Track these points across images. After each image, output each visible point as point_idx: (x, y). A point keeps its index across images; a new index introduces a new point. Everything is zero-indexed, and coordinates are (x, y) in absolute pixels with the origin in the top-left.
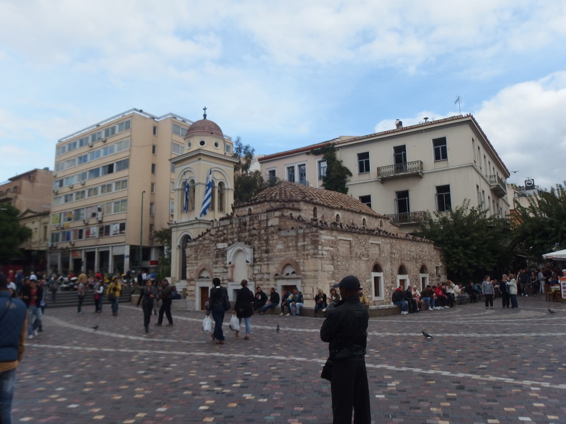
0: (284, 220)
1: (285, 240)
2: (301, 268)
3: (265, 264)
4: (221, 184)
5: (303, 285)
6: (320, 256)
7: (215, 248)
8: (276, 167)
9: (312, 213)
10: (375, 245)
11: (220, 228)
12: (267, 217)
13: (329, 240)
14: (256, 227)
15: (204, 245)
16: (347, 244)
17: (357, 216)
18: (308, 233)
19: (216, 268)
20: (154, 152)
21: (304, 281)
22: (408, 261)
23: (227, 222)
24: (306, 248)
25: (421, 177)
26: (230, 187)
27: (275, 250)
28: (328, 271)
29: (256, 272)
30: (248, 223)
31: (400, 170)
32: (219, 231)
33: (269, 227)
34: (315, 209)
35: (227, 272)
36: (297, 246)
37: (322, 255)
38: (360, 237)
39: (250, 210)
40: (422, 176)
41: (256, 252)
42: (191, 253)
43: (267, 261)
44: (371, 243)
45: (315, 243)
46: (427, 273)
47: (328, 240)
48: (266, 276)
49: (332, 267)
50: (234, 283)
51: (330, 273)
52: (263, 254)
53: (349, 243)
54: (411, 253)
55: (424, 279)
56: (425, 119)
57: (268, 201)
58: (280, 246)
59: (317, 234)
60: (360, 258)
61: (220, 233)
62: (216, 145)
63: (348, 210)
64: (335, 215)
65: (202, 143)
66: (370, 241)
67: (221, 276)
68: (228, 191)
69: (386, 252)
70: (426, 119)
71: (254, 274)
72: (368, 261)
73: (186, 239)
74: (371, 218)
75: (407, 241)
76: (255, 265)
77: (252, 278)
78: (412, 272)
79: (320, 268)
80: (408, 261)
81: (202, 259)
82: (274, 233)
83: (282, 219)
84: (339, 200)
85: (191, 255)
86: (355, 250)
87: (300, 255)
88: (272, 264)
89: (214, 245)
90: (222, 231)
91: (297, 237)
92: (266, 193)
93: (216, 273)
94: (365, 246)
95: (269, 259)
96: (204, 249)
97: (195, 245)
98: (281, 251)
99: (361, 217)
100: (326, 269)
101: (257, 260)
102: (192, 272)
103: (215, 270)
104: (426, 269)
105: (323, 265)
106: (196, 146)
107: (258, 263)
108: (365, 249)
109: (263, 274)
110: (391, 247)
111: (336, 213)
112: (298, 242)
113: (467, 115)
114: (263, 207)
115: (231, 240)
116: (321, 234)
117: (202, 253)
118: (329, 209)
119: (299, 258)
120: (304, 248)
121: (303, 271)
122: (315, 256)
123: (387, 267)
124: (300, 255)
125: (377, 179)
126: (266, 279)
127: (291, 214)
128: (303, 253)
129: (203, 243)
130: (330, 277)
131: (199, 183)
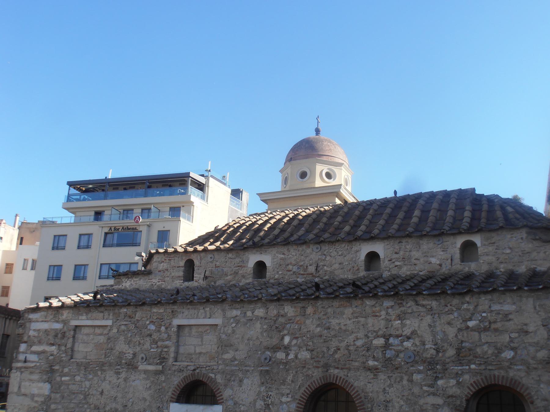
6: (19, 365)
13: (46, 332)
28: (33, 396)
38: (139, 314)
44: (179, 327)
51: (36, 399)
66: (177, 322)
79: (16, 390)
80: (374, 370)
86: (117, 348)
105: (23, 384)
111: (253, 258)
116: (30, 321)
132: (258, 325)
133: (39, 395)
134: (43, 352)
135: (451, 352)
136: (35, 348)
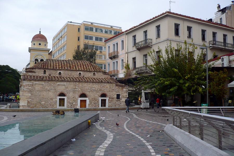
9: (43, 73)
20: (79, 40)
25: (151, 47)
28: (27, 96)
37: (24, 90)
62: (40, 44)
66: (57, 84)
79: (22, 95)
80: (89, 92)
116: (23, 82)
127: (45, 72)
132: (72, 85)
134: (28, 88)
135: (99, 90)
136: (25, 87)
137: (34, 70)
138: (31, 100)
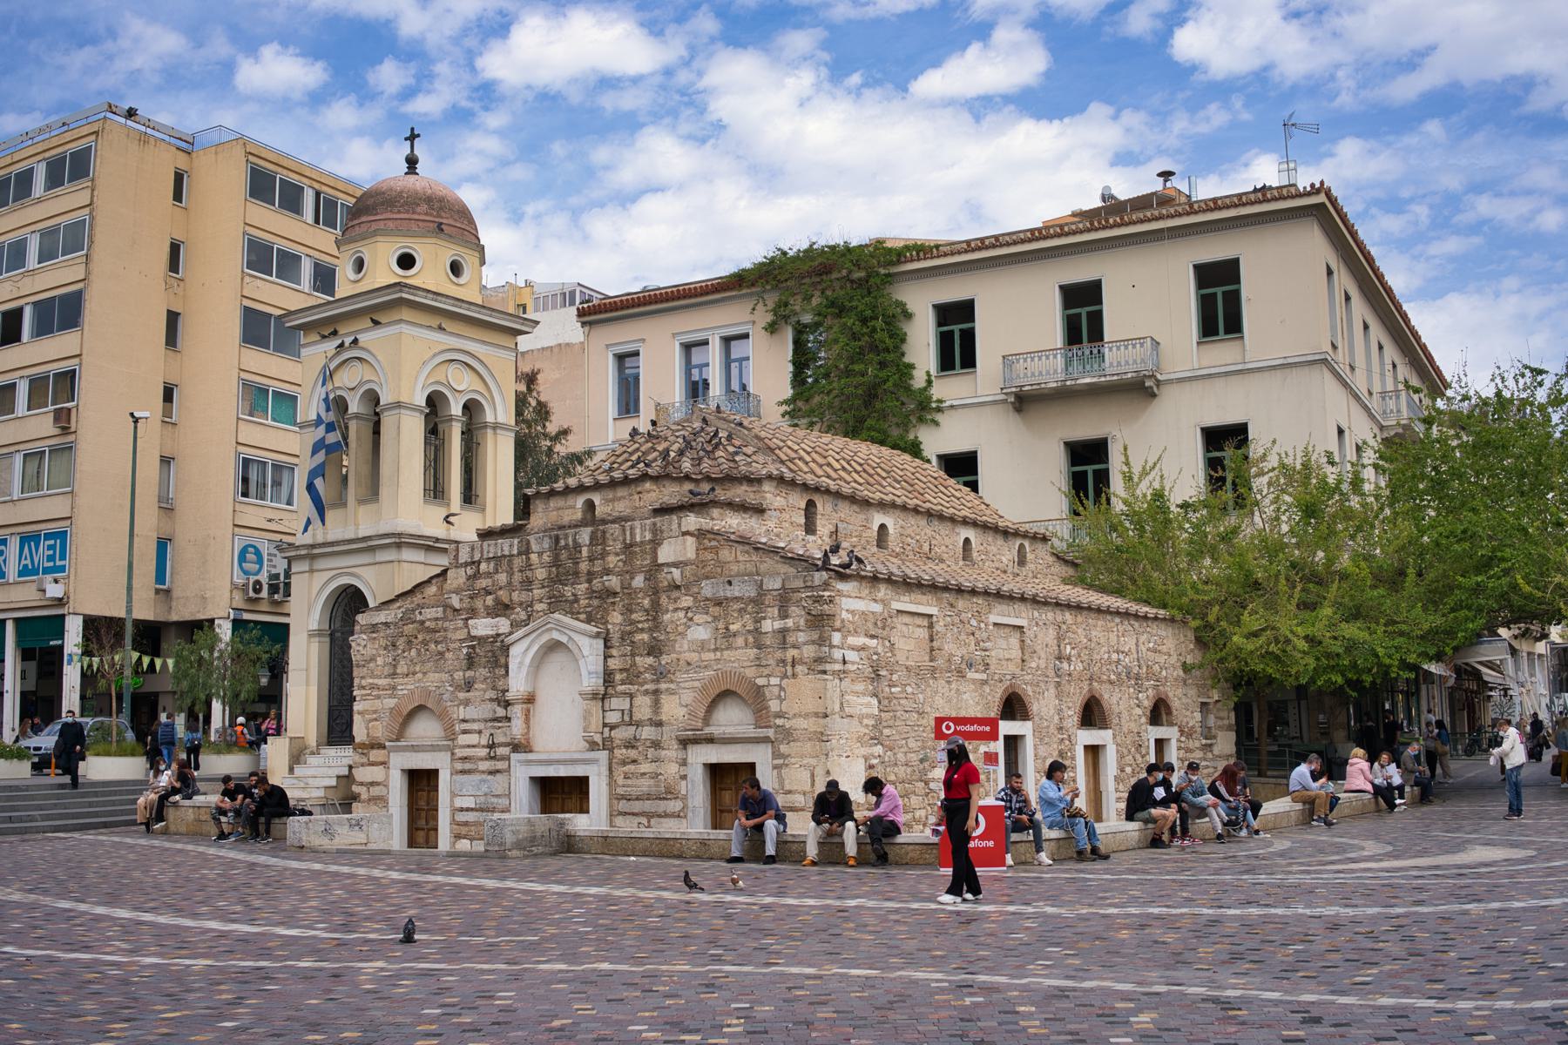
0: (714, 543)
1: (715, 610)
2: (774, 706)
3: (646, 692)
4: (471, 408)
5: (776, 762)
6: (838, 667)
7: (462, 634)
8: (643, 340)
9: (802, 521)
10: (1007, 630)
11: (483, 566)
12: (655, 530)
14: (615, 566)
15: (423, 623)
16: (919, 626)
17: (944, 529)
18: (797, 590)
19: (466, 703)
20: (174, 264)
21: (783, 748)
22: (1111, 682)
23: (508, 546)
24: (791, 639)
25: (1154, 395)
26: (501, 419)
27: (682, 645)
28: (861, 718)
29: (613, 718)
30: (585, 552)
31: (1081, 368)
32: (476, 576)
33: (663, 565)
34: (811, 504)
35: (508, 719)
36: (757, 631)
37: (845, 662)
38: (961, 604)
39: (590, 506)
40: (1155, 389)
41: (614, 652)
42: (374, 652)
43: (653, 681)
45: (820, 622)
46: (1171, 724)
47: (863, 613)
48: (647, 733)
49: (875, 701)
50: (530, 756)
51: (866, 721)
52: (637, 658)
53: (925, 623)
54: (1121, 657)
55: (1160, 744)
56: (1160, 175)
57: (656, 479)
58: (700, 633)
59: (827, 594)
60: (961, 674)
61: (483, 583)
63: (916, 511)
64: (876, 528)
65: (406, 261)
67: (486, 734)
68: (495, 434)
69: (1043, 656)
70: (1166, 175)
71: (605, 725)
72: (984, 682)
73: (349, 602)
74: (990, 537)
75: (1109, 617)
76: (612, 696)
77: (598, 738)
78: (1123, 721)
79: (837, 708)
80: (1111, 682)
81: (414, 673)
82: (678, 587)
83: (706, 541)
84: (884, 474)
85: (373, 659)
87: (771, 662)
88: (672, 693)
89: (460, 624)
90: (488, 575)
91: (758, 601)
92: (643, 449)
93: (464, 721)
94: (978, 633)
95: (661, 675)
96: (420, 637)
97: (386, 624)
98: (702, 646)
99: (958, 534)
100: (856, 711)
101: (618, 677)
102: (376, 720)
103: (462, 712)
104: (1169, 712)
105: (847, 697)
106: (383, 271)
107: (620, 688)
108: (977, 643)
109: (638, 724)
110: (1059, 639)
111: (878, 518)
112: (764, 618)
113: (1312, 185)
114: (636, 497)
115: (525, 609)
116: (840, 593)
117: (413, 653)
118: (855, 507)
119: (766, 672)
120: (784, 637)
121: (780, 715)
122: (820, 668)
123: (1044, 704)
124: (771, 662)
125: (1003, 397)
126: (648, 744)
128: (779, 654)
129: (419, 618)
130: (867, 737)
131: (398, 405)
133: (868, 716)
137: (740, 493)
138: (879, 750)
